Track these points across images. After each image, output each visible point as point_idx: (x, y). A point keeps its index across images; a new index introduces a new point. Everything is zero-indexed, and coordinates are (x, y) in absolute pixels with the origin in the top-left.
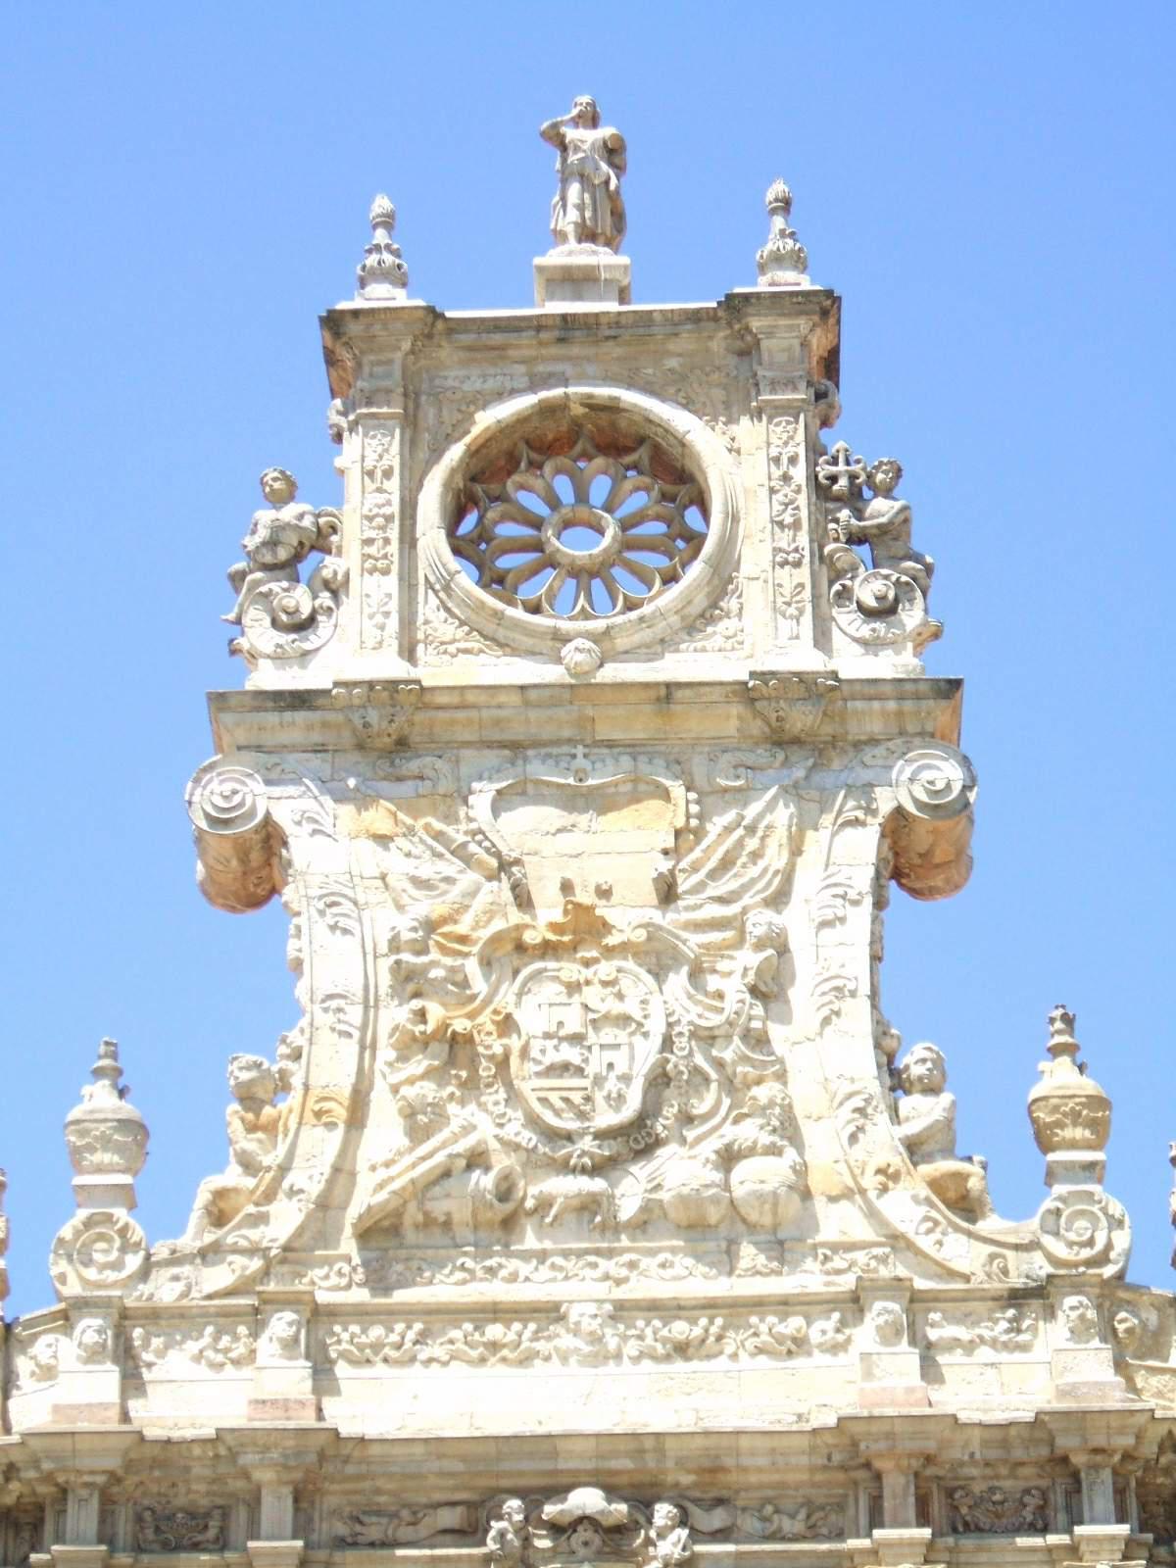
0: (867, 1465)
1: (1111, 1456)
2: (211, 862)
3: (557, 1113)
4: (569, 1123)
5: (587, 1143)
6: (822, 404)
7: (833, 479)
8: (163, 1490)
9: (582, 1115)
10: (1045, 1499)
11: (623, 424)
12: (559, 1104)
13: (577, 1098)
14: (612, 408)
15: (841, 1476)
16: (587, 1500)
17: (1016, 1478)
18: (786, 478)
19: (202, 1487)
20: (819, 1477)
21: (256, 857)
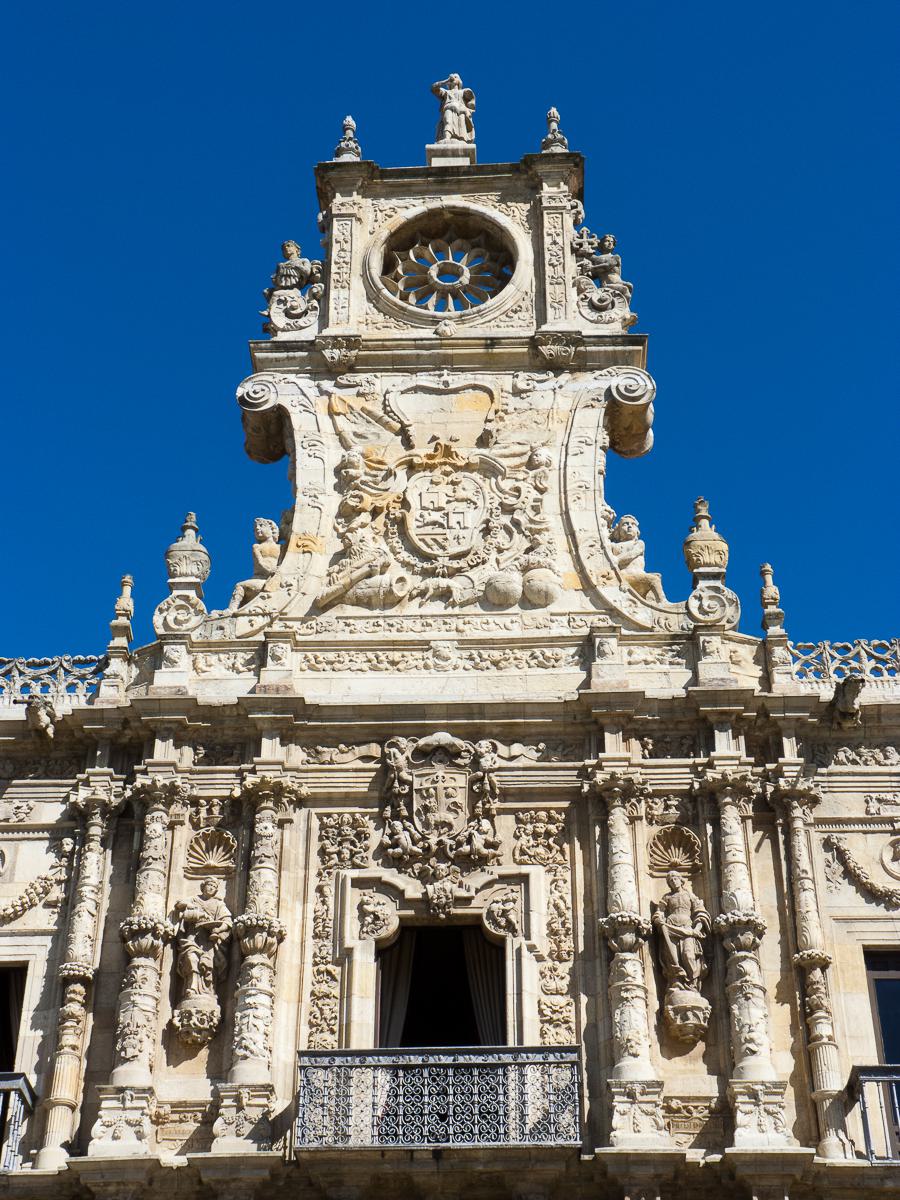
0: (596, 722)
1: (731, 716)
2: (250, 431)
3: (428, 546)
4: (437, 551)
5: (446, 561)
6: (574, 211)
7: (581, 245)
8: (209, 734)
9: (443, 548)
10: (695, 742)
11: (471, 223)
12: (431, 542)
13: (440, 539)
14: (464, 213)
15: (581, 729)
16: (443, 738)
17: (678, 730)
18: (555, 243)
19: (230, 732)
20: (569, 729)
21: (273, 428)
